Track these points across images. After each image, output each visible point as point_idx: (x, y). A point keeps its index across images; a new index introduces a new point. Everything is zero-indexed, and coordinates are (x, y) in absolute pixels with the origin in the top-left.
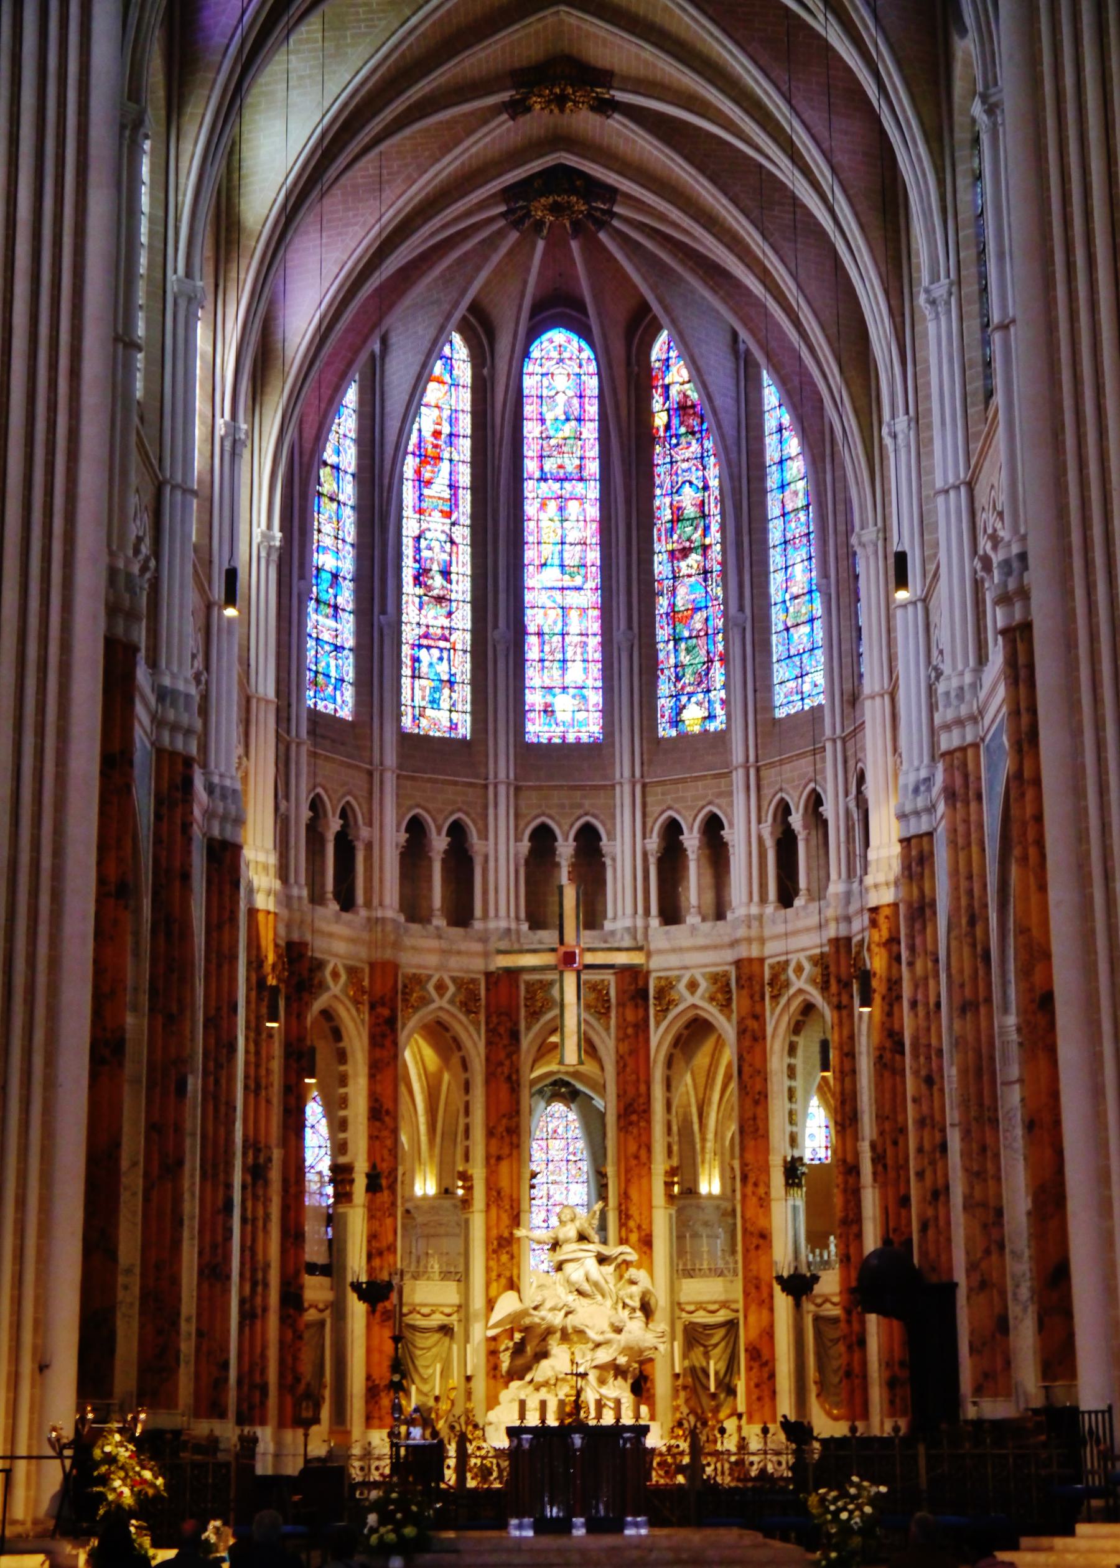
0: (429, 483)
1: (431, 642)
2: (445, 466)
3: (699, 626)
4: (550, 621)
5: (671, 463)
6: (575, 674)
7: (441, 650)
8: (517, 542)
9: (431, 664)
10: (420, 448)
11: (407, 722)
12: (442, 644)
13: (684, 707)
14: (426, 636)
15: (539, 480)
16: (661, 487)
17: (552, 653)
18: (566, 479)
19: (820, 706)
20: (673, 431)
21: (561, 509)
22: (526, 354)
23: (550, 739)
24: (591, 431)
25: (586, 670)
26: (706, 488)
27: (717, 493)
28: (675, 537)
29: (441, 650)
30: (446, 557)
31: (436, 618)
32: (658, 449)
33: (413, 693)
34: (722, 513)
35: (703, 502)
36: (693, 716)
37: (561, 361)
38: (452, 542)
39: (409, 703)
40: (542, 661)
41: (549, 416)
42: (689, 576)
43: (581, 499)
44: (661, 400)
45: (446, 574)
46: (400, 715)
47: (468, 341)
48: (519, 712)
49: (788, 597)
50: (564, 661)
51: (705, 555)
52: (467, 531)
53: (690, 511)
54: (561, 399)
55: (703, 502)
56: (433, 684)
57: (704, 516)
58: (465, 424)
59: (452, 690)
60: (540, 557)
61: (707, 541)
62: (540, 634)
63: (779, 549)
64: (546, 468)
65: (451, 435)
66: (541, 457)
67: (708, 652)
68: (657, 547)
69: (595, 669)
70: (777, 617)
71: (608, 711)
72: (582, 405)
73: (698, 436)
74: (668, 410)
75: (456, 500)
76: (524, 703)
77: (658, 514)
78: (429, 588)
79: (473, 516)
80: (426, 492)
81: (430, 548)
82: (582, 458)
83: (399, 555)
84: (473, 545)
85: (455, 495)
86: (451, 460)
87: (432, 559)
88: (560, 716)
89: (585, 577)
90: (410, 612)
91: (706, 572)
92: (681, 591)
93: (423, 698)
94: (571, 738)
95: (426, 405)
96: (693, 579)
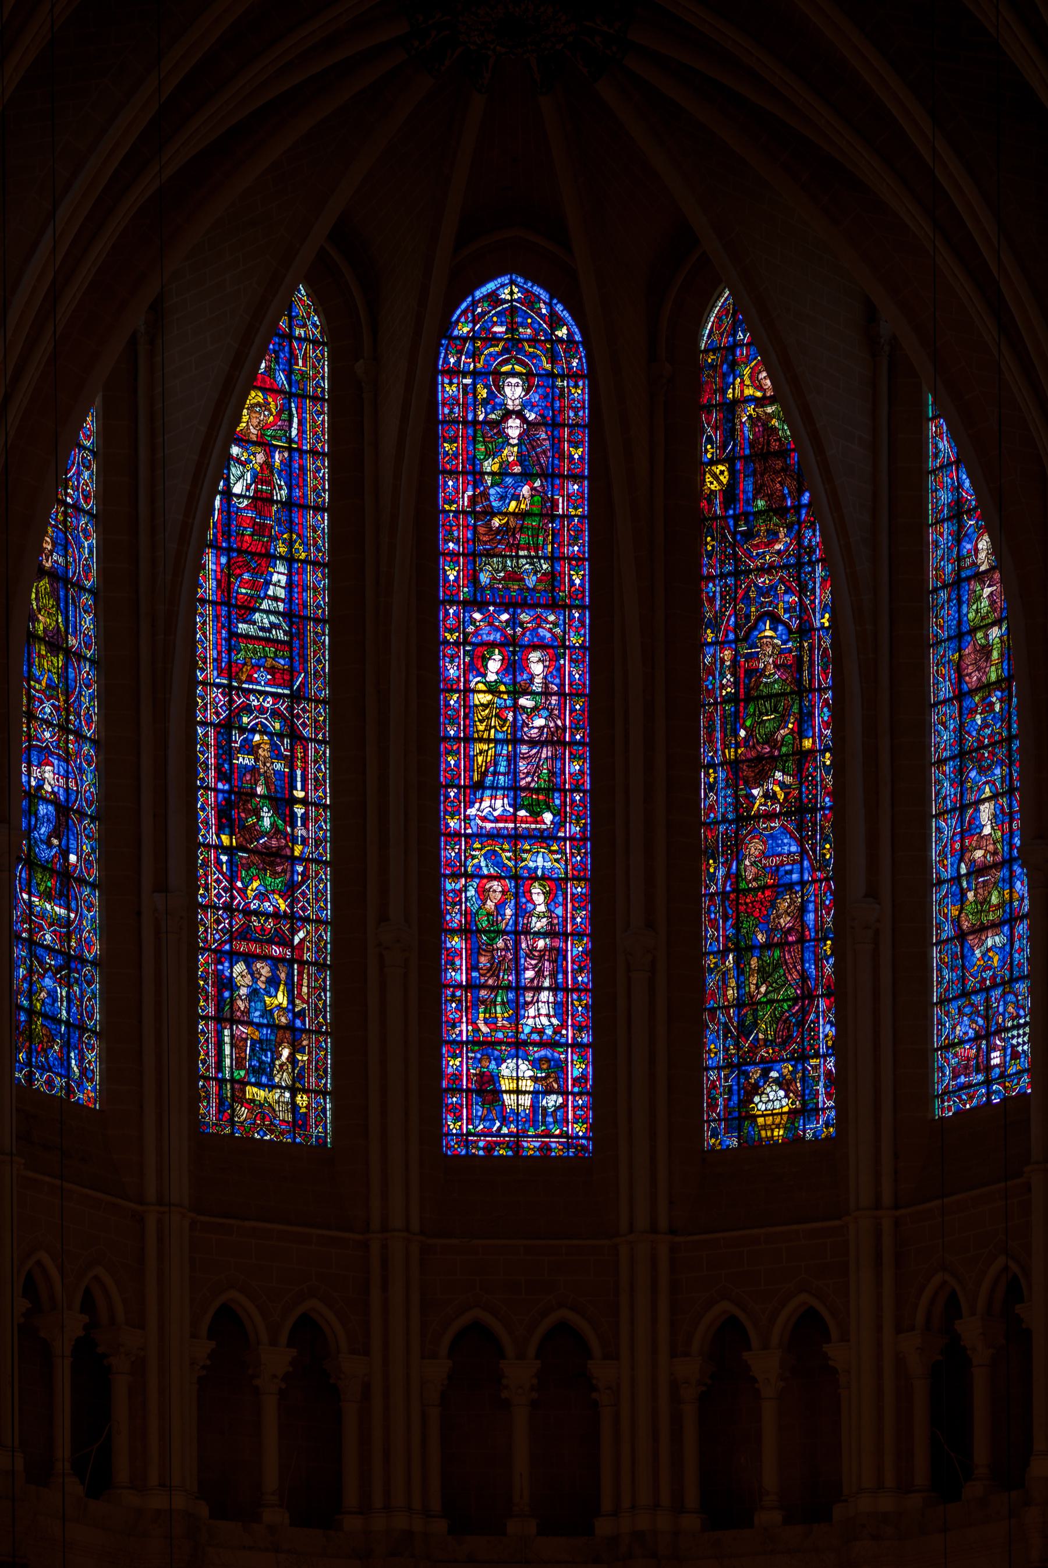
0: (247, 610)
1: (253, 947)
2: (279, 575)
3: (785, 921)
4: (490, 905)
5: (736, 574)
6: (539, 1014)
7: (275, 962)
8: (427, 741)
9: (254, 994)
10: (227, 534)
11: (209, 1110)
12: (276, 951)
13: (756, 1089)
14: (245, 934)
15: (469, 605)
16: (715, 626)
17: (494, 970)
18: (525, 605)
19: (1022, 1095)
20: (740, 507)
21: (514, 666)
22: (446, 327)
23: (489, 1148)
24: (571, 499)
25: (560, 1009)
26: (805, 630)
27: (827, 642)
28: (743, 733)
29: (275, 962)
30: (278, 766)
31: (262, 896)
32: (710, 543)
33: (221, 1051)
34: (837, 687)
35: (799, 659)
36: (773, 1101)
37: (513, 345)
38: (296, 737)
39: (212, 1073)
40: (471, 986)
41: (490, 465)
42: (770, 816)
43: (554, 650)
44: (718, 437)
45: (283, 803)
46: (195, 1099)
47: (321, 301)
48: (430, 1093)
49: (963, 870)
50: (519, 989)
51: (799, 774)
52: (323, 713)
53: (774, 679)
54: (514, 428)
55: (799, 659)
56: (257, 1035)
57: (801, 691)
58: (318, 476)
59: (296, 1049)
60: (469, 769)
61: (807, 744)
62: (468, 931)
63: (947, 769)
64: (484, 578)
65: (288, 504)
66: (473, 557)
67: (804, 977)
68: (706, 755)
69: (579, 1005)
70: (944, 913)
71: (604, 1095)
72: (556, 443)
73: (791, 518)
74: (730, 461)
75: (303, 647)
76: (438, 1072)
77: (709, 683)
78: (253, 832)
79: (335, 680)
80: (242, 627)
81: (251, 749)
82: (552, 559)
83: (191, 763)
84: (333, 742)
85: (302, 635)
86: (290, 560)
87: (253, 770)
88: (509, 1100)
89: (560, 813)
90: (213, 887)
91: (799, 811)
92: (755, 847)
93: (239, 1064)
94: (531, 1146)
95: (243, 441)
96: (776, 824)
